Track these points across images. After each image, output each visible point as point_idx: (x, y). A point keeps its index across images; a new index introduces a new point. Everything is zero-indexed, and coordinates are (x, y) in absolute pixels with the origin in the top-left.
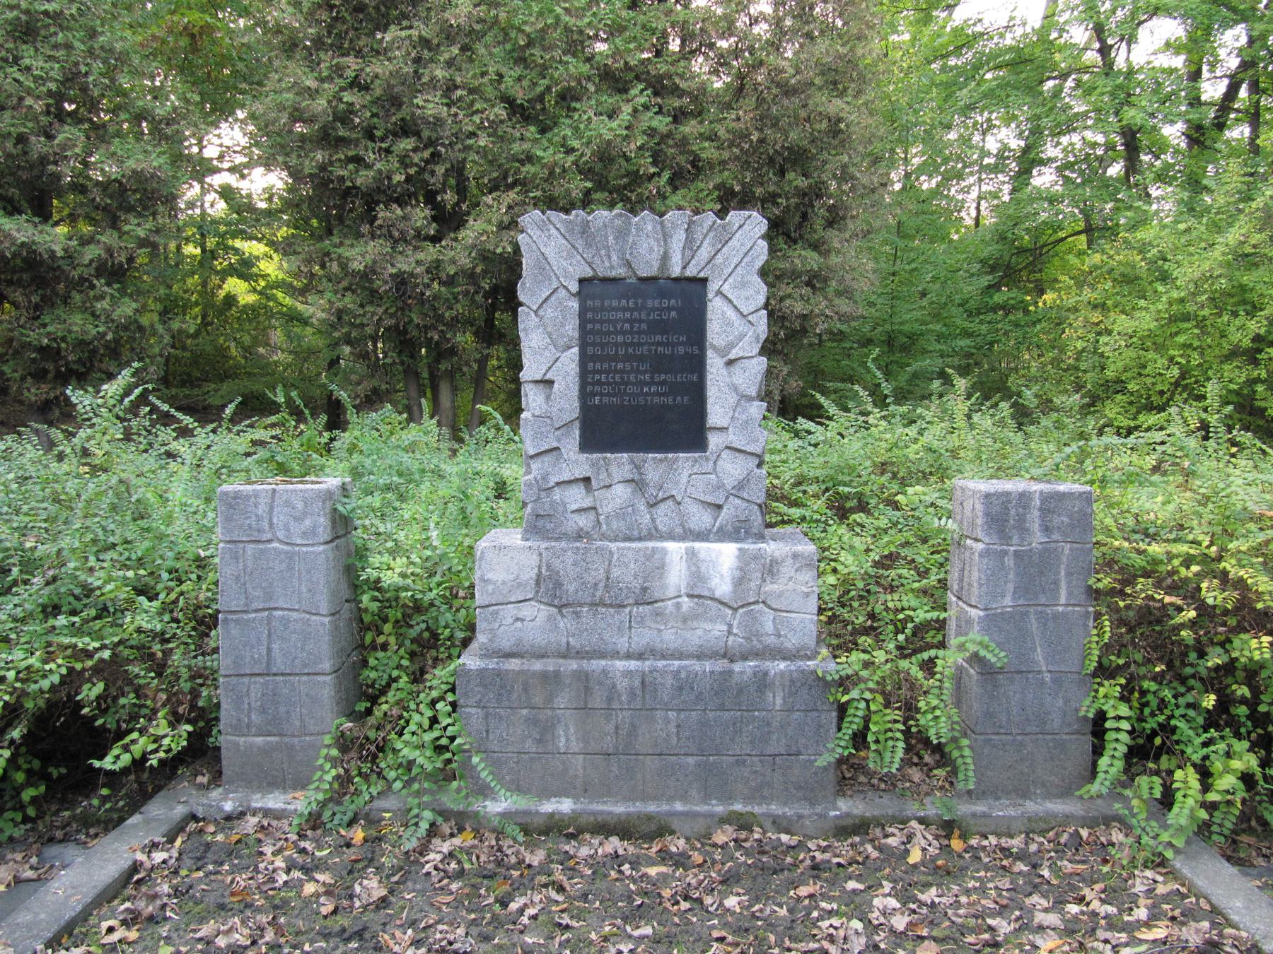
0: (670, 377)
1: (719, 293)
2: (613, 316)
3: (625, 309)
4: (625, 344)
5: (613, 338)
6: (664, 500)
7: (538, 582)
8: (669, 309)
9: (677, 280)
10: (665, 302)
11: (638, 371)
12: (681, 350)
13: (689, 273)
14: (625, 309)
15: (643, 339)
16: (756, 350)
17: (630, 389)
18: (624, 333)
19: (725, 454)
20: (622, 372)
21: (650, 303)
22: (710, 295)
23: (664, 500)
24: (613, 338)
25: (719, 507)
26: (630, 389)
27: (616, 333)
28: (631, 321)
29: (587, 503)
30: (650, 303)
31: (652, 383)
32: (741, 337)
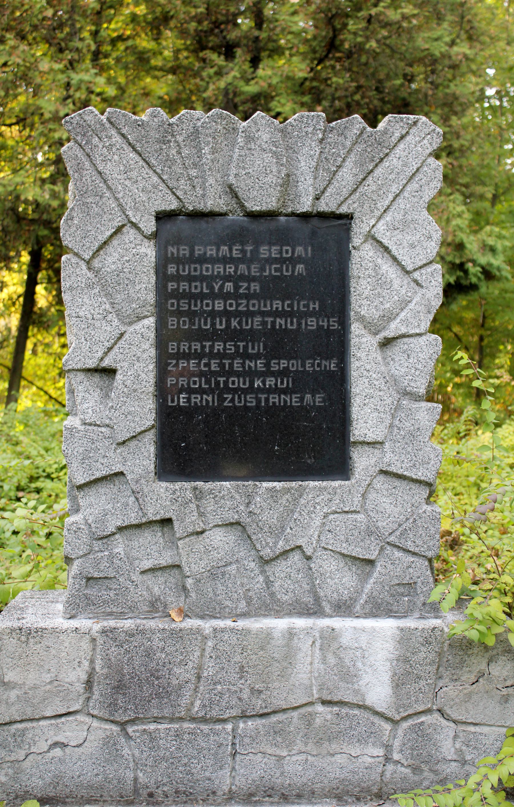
0: (294, 365)
1: (371, 237)
2: (207, 269)
3: (225, 261)
4: (226, 314)
5: (207, 305)
6: (285, 553)
7: (89, 684)
8: (293, 261)
9: (305, 216)
10: (287, 251)
11: (246, 356)
12: (312, 323)
13: (323, 207)
14: (225, 261)
15: (254, 305)
16: (425, 324)
17: (235, 382)
18: (225, 296)
19: (380, 482)
20: (222, 356)
21: (264, 251)
22: (356, 240)
23: (285, 553)
24: (207, 305)
25: (371, 562)
26: (235, 382)
27: (213, 296)
28: (236, 279)
29: (165, 560)
30: (264, 251)
31: (268, 373)
32: (405, 303)
